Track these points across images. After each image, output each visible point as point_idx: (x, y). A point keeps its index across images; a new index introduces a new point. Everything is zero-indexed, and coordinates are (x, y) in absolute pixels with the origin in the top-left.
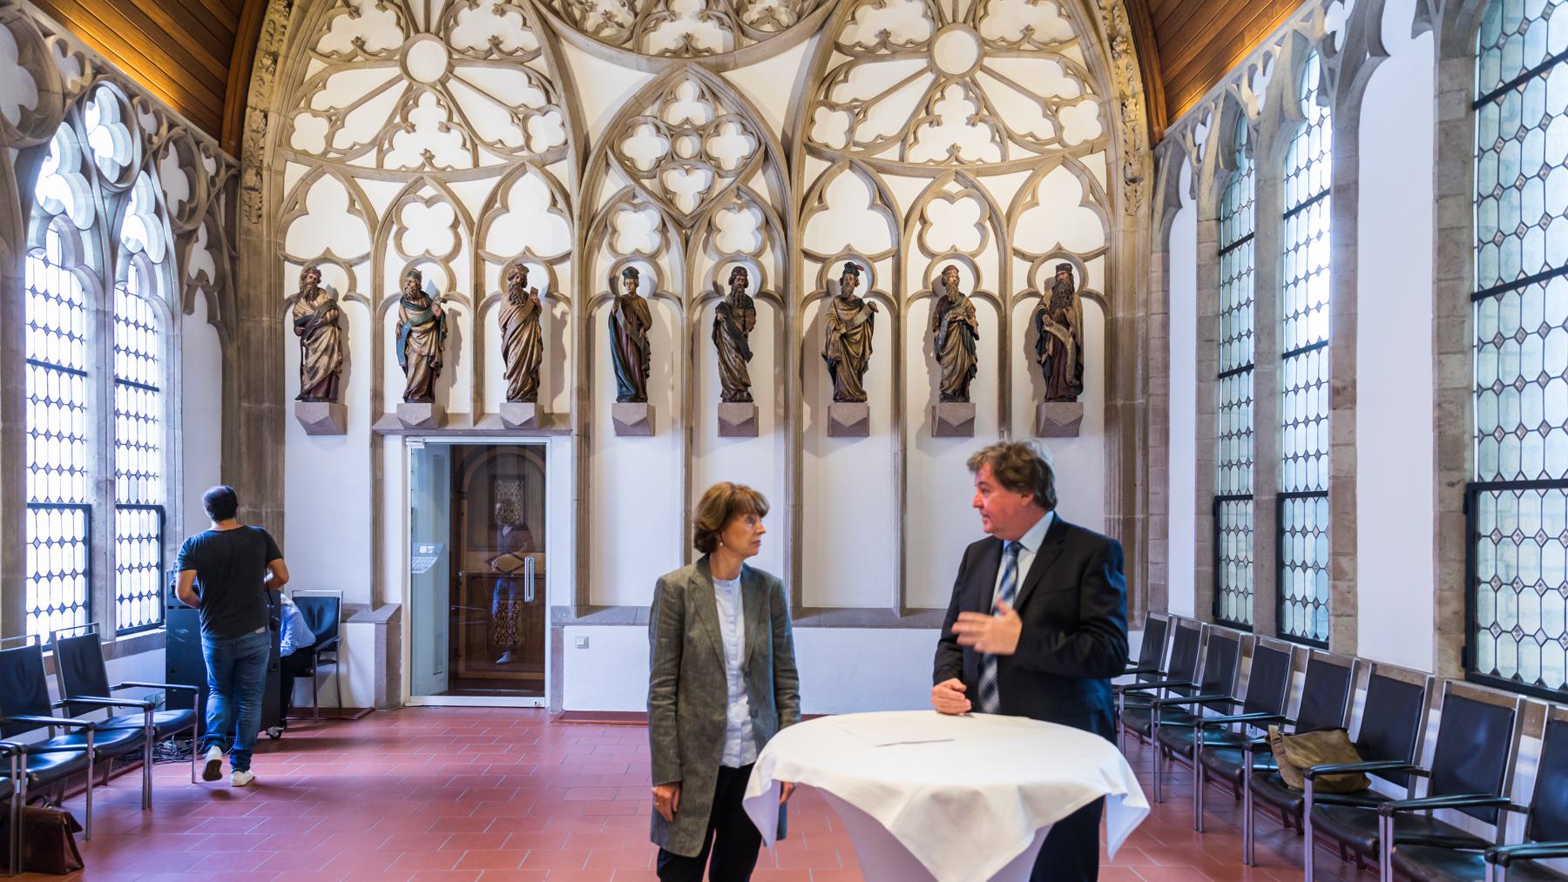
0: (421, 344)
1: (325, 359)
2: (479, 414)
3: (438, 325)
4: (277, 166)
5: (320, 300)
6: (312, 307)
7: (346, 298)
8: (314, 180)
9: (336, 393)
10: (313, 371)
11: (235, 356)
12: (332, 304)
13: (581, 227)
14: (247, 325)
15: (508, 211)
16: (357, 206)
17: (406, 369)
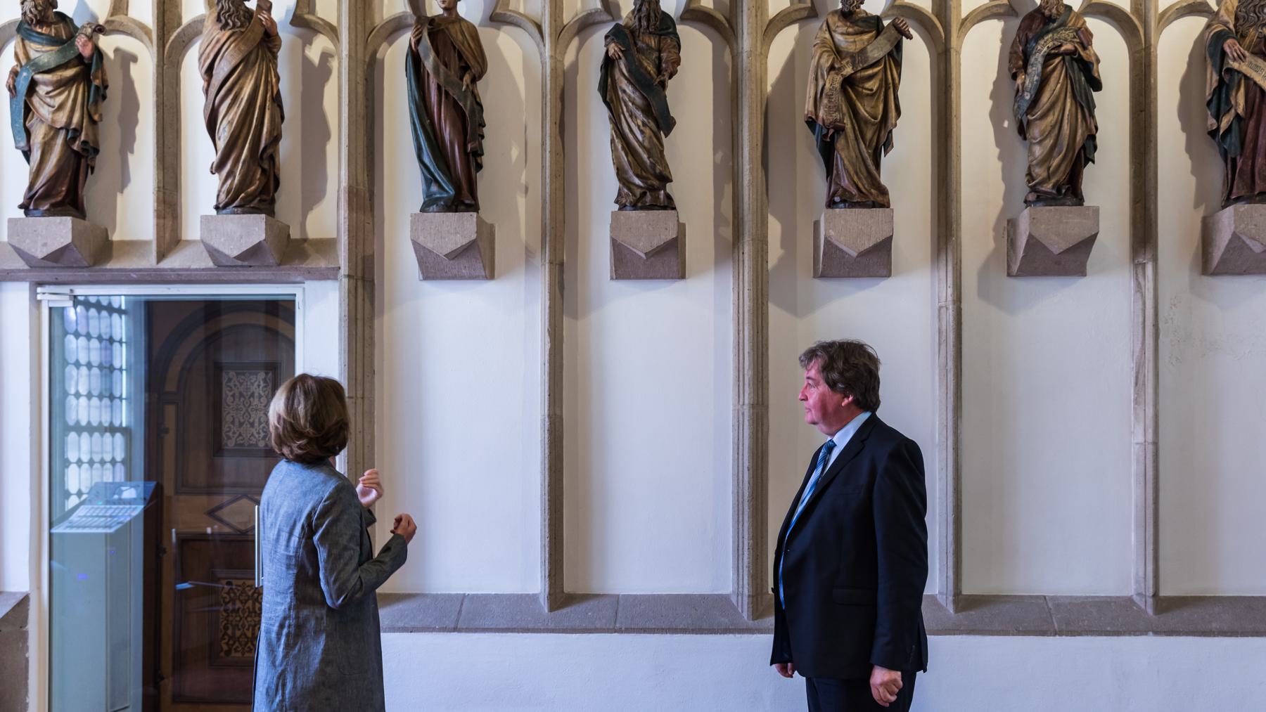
0: (53, 108)
2: (170, 238)
3: (88, 73)
17: (27, 155)
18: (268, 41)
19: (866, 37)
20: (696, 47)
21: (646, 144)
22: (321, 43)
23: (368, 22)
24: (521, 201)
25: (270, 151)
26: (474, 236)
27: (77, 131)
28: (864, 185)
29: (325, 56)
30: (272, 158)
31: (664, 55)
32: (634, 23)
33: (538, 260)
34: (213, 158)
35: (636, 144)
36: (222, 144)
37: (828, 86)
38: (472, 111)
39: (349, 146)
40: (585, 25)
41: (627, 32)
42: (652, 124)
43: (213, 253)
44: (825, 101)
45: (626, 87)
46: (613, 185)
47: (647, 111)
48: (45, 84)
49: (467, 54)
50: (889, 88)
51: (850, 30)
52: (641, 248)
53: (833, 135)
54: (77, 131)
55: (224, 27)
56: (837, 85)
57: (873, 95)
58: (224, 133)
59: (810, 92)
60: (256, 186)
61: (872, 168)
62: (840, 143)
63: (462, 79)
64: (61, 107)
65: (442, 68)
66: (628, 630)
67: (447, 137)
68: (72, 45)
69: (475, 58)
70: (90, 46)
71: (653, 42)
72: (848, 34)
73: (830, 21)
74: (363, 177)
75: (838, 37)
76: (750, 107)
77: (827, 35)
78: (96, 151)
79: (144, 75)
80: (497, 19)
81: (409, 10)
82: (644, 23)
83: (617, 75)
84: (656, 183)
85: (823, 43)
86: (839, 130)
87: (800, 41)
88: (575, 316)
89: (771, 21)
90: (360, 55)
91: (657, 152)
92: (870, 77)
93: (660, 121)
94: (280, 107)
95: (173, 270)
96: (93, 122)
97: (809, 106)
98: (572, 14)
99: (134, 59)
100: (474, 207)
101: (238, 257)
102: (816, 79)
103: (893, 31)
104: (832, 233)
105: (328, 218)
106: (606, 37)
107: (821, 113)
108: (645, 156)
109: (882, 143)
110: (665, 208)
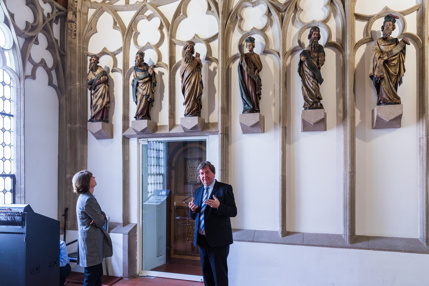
0: (143, 90)
1: (101, 100)
2: (172, 125)
3: (152, 79)
4: (84, 10)
5: (98, 71)
6: (95, 75)
7: (113, 71)
8: (100, 15)
9: (107, 117)
10: (95, 106)
11: (64, 102)
12: (105, 73)
13: (223, 18)
14: (70, 87)
15: (186, 17)
16: (118, 25)
17: (136, 103)
18: (199, 65)
19: (392, 46)
20: (330, 55)
21: (314, 88)
22: (214, 64)
23: (227, 57)
24: (273, 108)
25: (199, 98)
26: (258, 120)
27: (149, 96)
28: (391, 97)
29: (215, 68)
30: (200, 100)
31: (320, 59)
32: (309, 49)
33: (278, 126)
34: (184, 101)
35: (310, 88)
36: (186, 97)
37: (378, 64)
38: (258, 81)
39: (221, 95)
40: (293, 51)
41: (307, 52)
42: (316, 81)
43: (184, 128)
44: (377, 69)
45: (307, 70)
46: (302, 102)
47: (314, 77)
48: (141, 83)
49: (256, 64)
50: (401, 62)
51: (386, 44)
52: (312, 121)
53: (380, 81)
54: (149, 96)
55: (187, 63)
56: (382, 63)
57: (395, 65)
58: (187, 93)
59: (372, 66)
60: (195, 109)
61: (395, 91)
62: (383, 83)
63: (255, 72)
64: (145, 89)
65: (249, 69)
66: (308, 245)
67: (250, 90)
68: (148, 71)
69: (259, 65)
70: (152, 71)
71: (316, 55)
72: (385, 45)
73: (379, 42)
74: (225, 103)
75: (382, 47)
76: (349, 73)
77: (378, 47)
78: (154, 101)
79: (166, 79)
80: (265, 52)
81: (239, 52)
82: (313, 49)
83: (304, 66)
84: (317, 100)
85: (376, 49)
86: (382, 78)
87: (367, 50)
88: (290, 144)
89: (356, 44)
90: (225, 67)
91: (317, 90)
92: (394, 60)
93: (319, 80)
94: (202, 84)
95: (173, 133)
96: (153, 93)
97: (371, 71)
98: (289, 48)
99: (163, 74)
100: (258, 111)
101: (191, 129)
102: (374, 62)
103: (403, 43)
104: (380, 114)
105: (215, 117)
106: (300, 55)
107: (376, 73)
108: (313, 92)
109: (398, 81)
110: (320, 108)
